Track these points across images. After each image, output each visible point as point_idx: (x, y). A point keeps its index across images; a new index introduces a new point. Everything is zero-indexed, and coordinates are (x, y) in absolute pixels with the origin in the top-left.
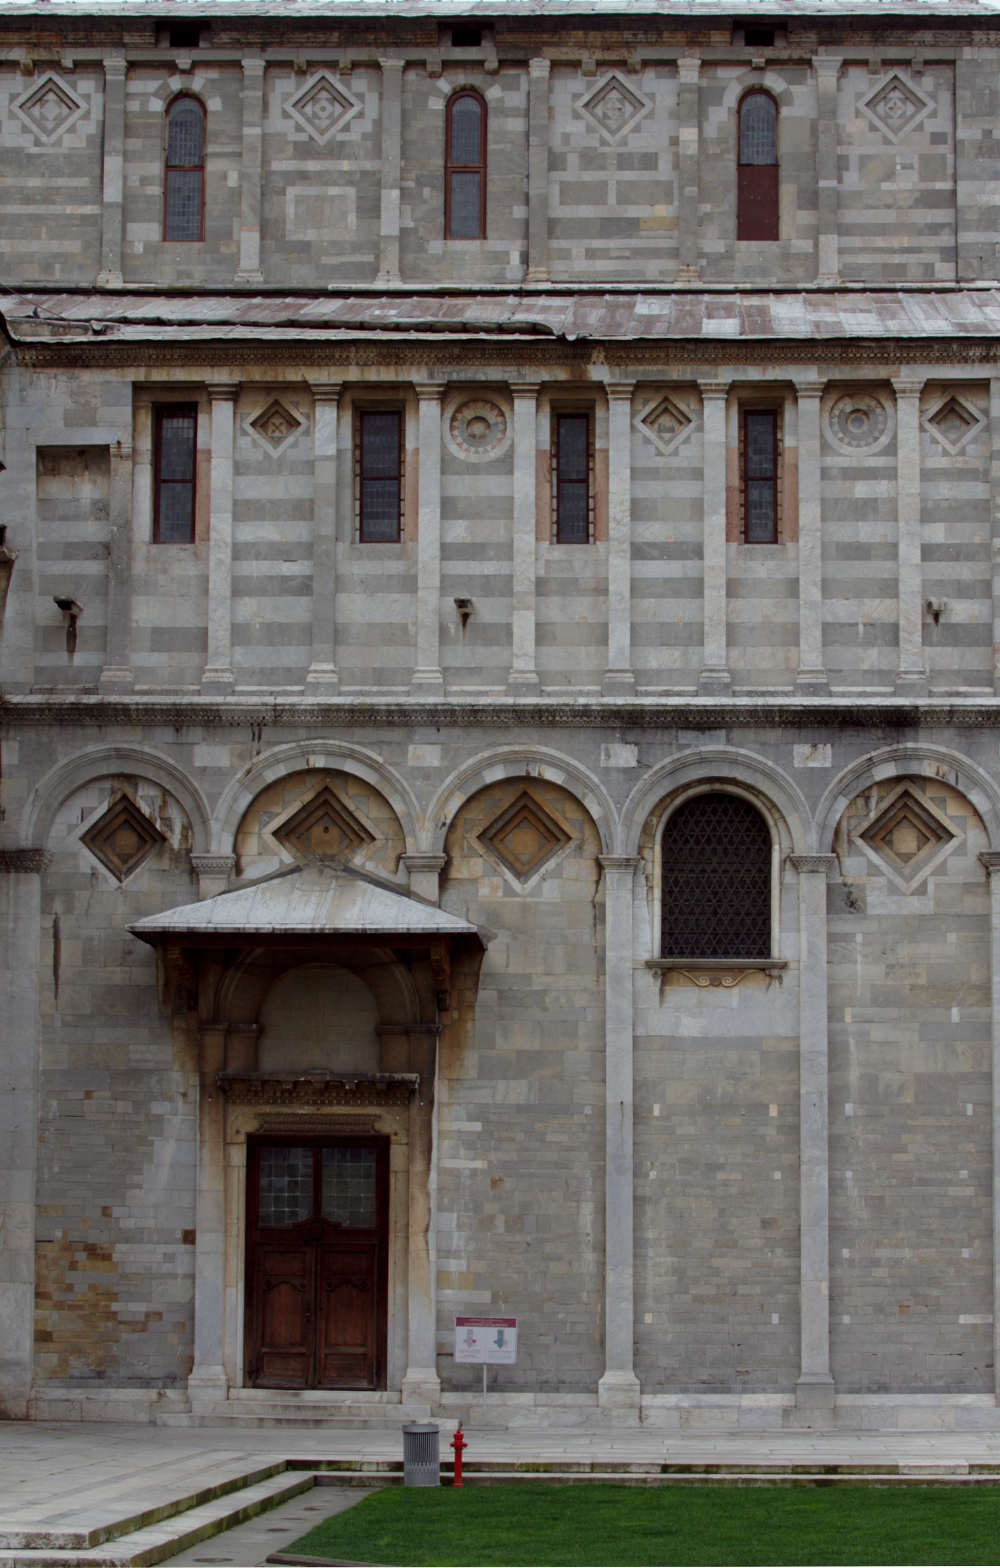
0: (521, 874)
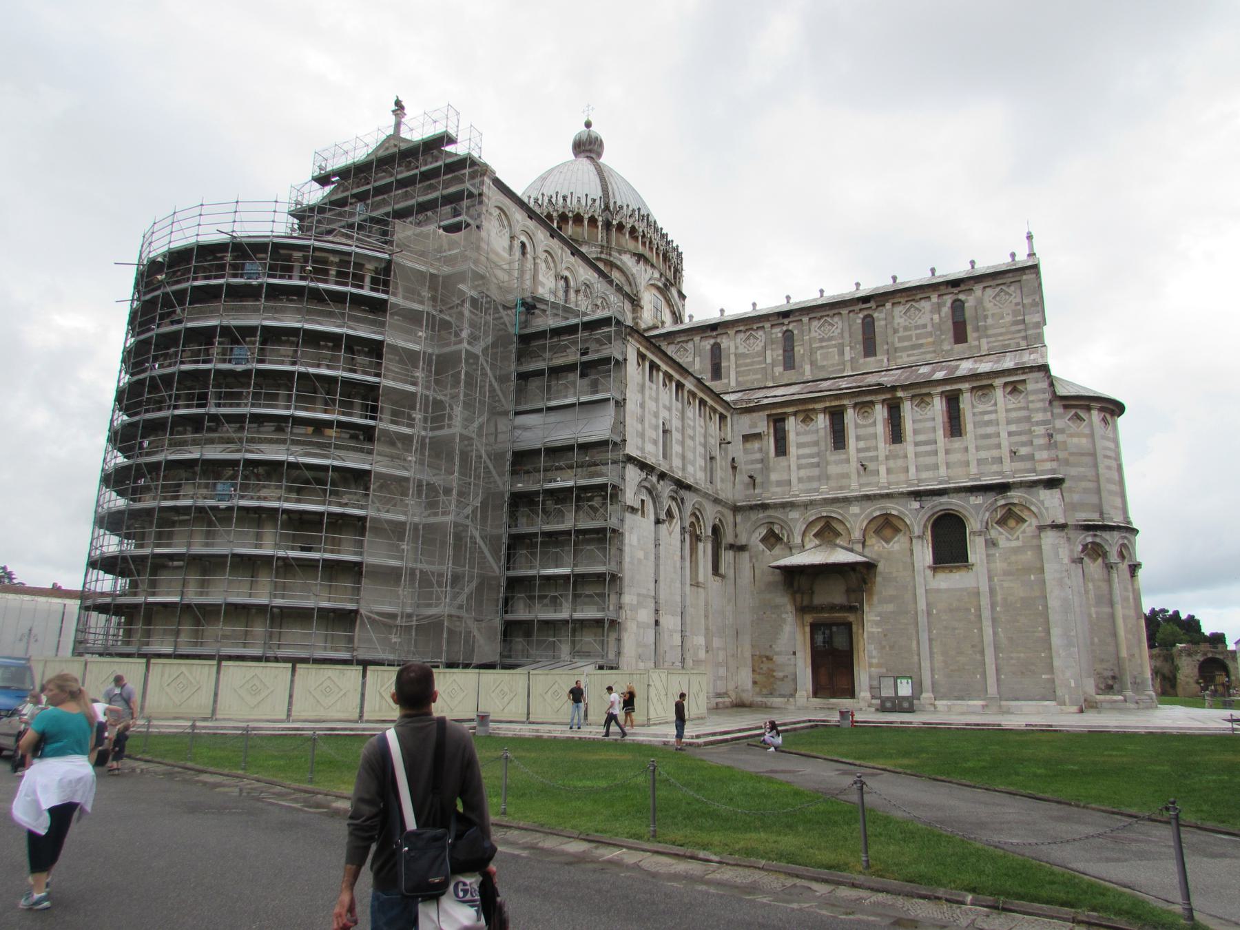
0: (887, 542)
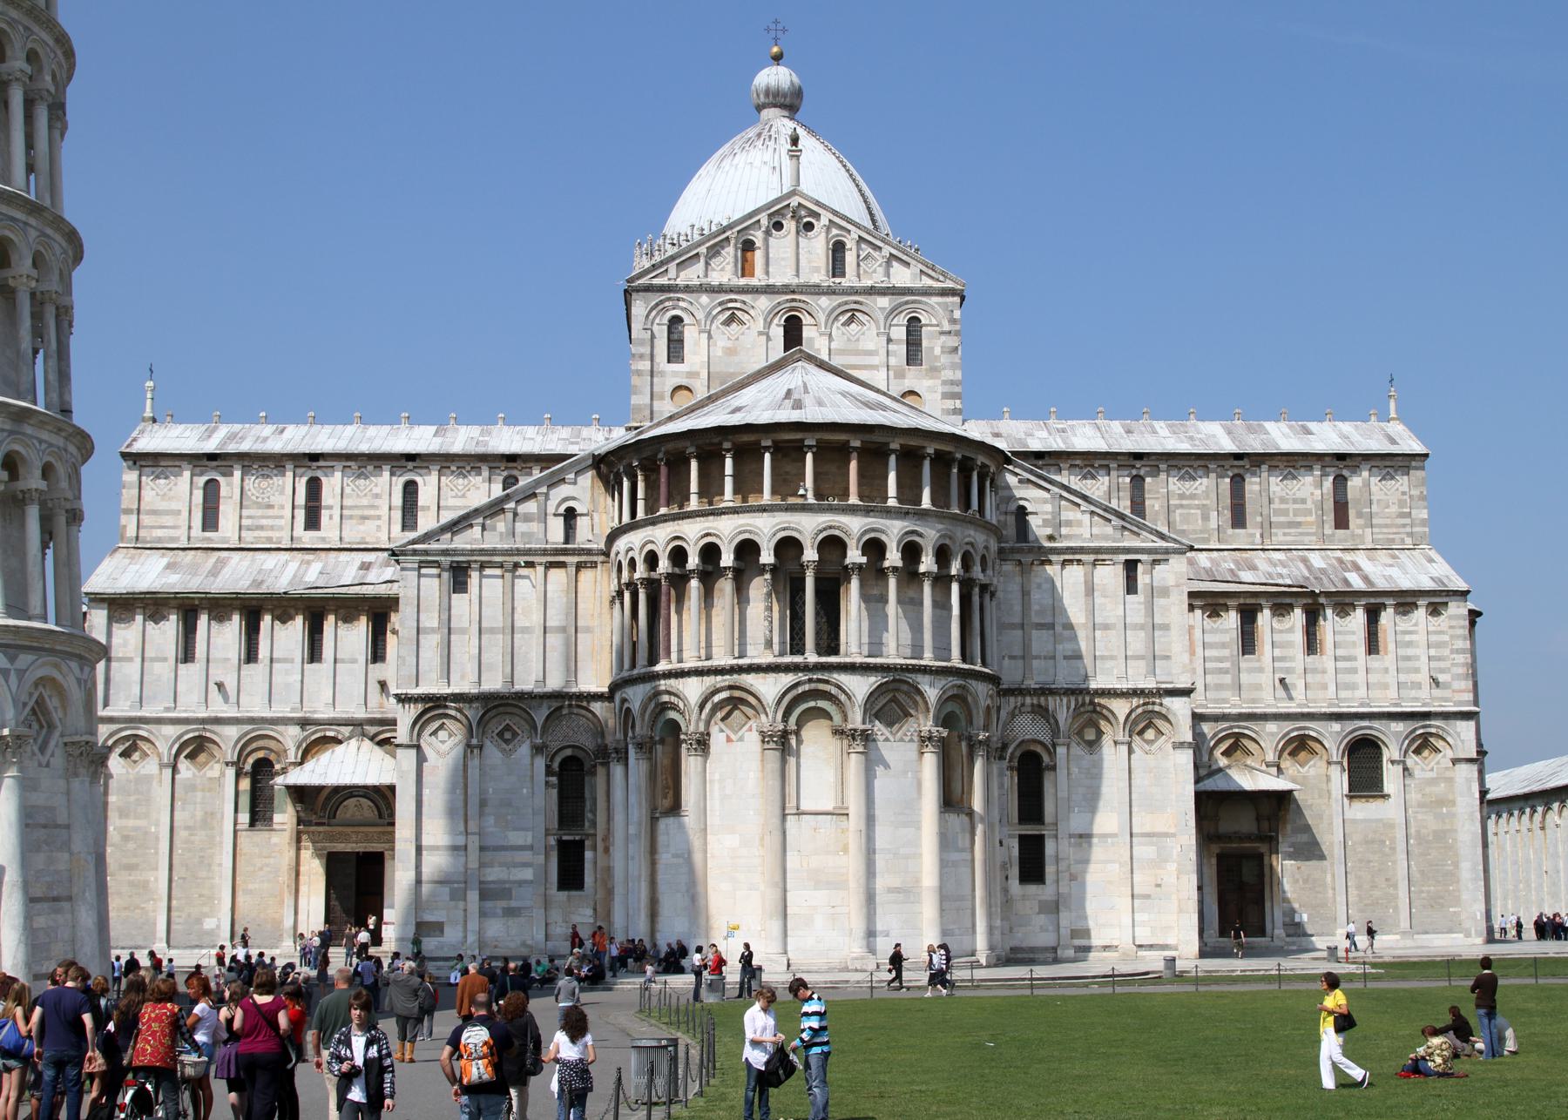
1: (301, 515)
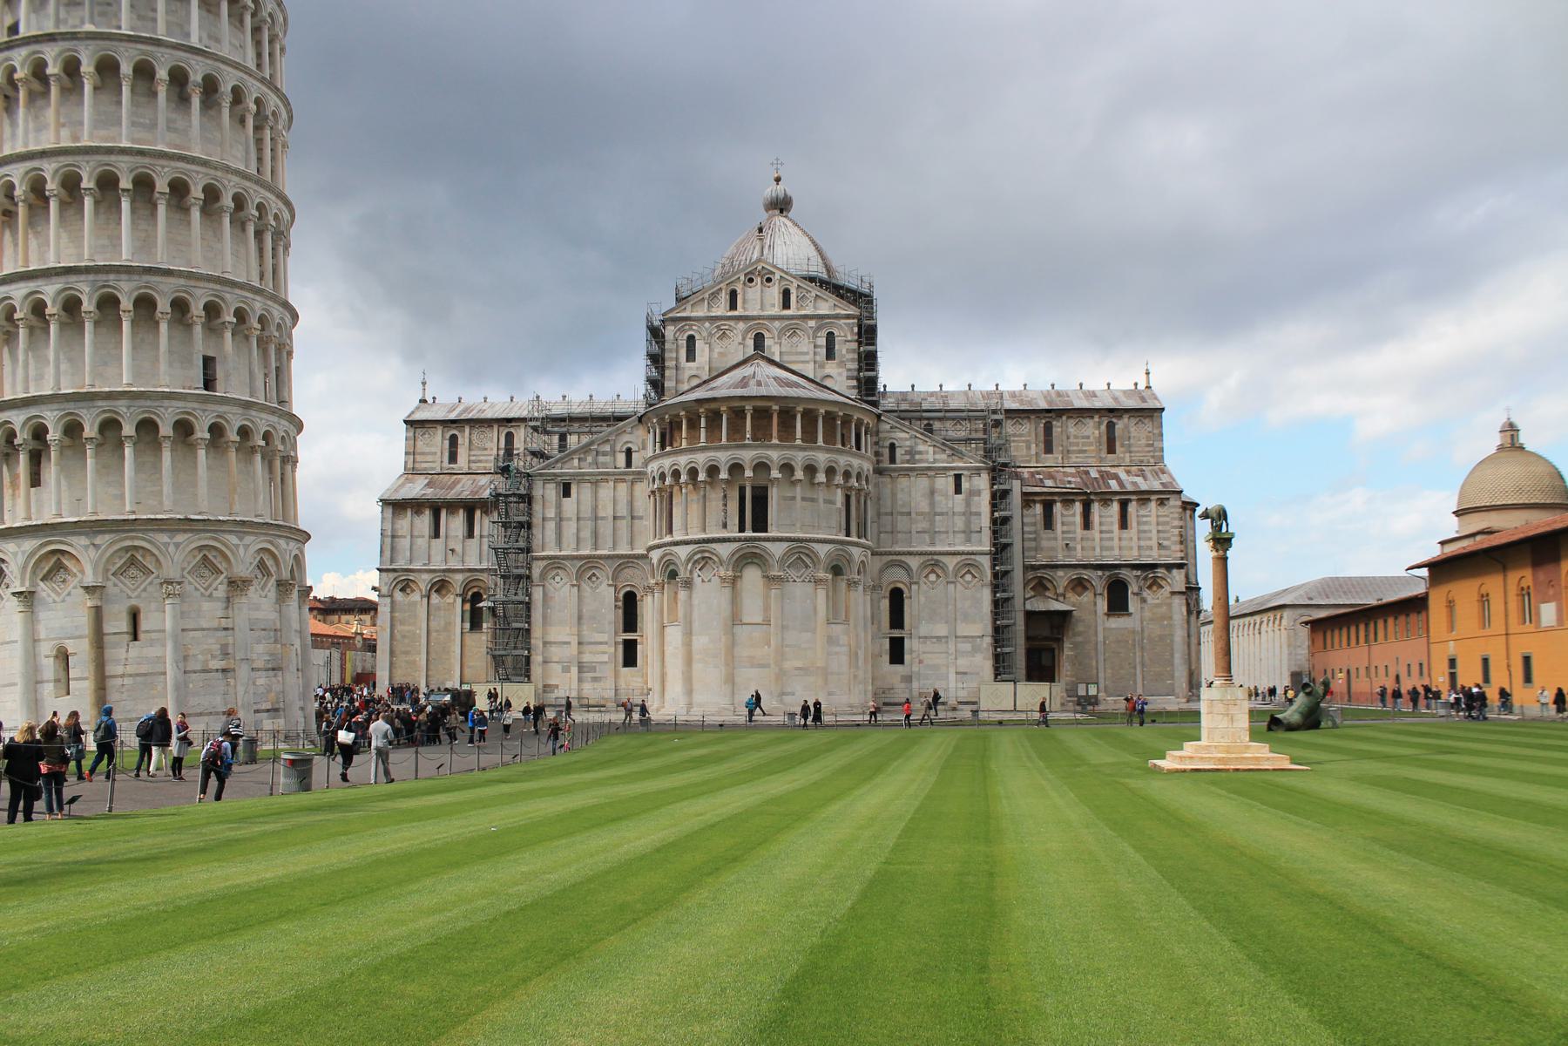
0: (1079, 596)
1: (446, 455)
